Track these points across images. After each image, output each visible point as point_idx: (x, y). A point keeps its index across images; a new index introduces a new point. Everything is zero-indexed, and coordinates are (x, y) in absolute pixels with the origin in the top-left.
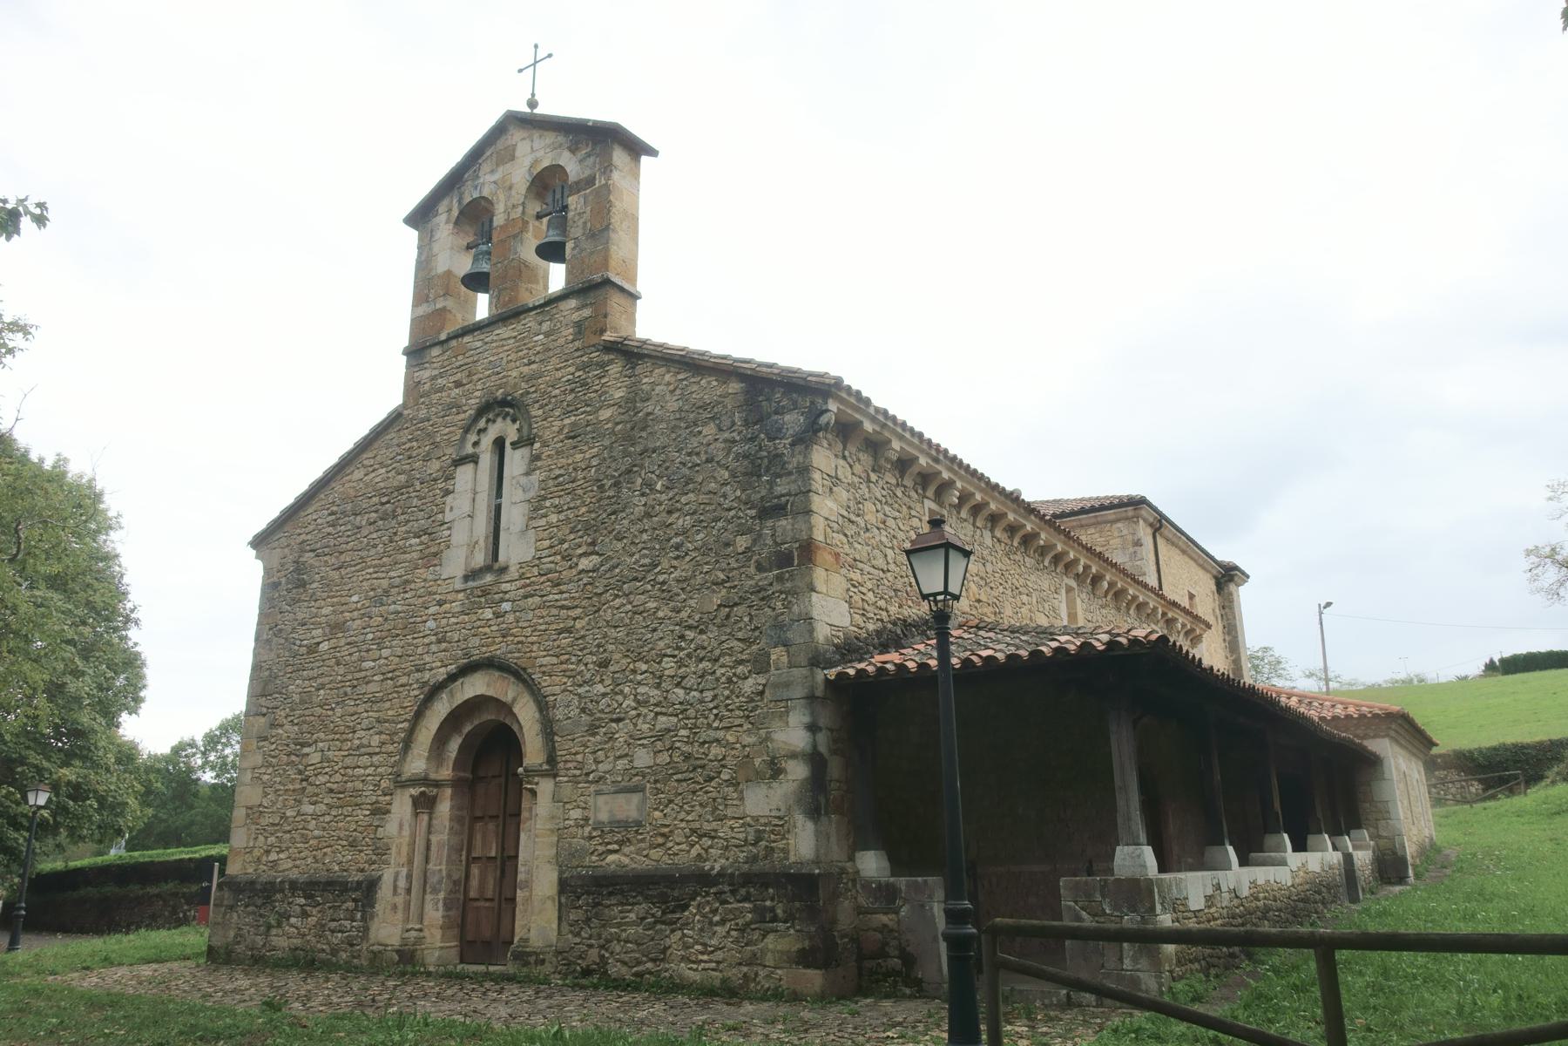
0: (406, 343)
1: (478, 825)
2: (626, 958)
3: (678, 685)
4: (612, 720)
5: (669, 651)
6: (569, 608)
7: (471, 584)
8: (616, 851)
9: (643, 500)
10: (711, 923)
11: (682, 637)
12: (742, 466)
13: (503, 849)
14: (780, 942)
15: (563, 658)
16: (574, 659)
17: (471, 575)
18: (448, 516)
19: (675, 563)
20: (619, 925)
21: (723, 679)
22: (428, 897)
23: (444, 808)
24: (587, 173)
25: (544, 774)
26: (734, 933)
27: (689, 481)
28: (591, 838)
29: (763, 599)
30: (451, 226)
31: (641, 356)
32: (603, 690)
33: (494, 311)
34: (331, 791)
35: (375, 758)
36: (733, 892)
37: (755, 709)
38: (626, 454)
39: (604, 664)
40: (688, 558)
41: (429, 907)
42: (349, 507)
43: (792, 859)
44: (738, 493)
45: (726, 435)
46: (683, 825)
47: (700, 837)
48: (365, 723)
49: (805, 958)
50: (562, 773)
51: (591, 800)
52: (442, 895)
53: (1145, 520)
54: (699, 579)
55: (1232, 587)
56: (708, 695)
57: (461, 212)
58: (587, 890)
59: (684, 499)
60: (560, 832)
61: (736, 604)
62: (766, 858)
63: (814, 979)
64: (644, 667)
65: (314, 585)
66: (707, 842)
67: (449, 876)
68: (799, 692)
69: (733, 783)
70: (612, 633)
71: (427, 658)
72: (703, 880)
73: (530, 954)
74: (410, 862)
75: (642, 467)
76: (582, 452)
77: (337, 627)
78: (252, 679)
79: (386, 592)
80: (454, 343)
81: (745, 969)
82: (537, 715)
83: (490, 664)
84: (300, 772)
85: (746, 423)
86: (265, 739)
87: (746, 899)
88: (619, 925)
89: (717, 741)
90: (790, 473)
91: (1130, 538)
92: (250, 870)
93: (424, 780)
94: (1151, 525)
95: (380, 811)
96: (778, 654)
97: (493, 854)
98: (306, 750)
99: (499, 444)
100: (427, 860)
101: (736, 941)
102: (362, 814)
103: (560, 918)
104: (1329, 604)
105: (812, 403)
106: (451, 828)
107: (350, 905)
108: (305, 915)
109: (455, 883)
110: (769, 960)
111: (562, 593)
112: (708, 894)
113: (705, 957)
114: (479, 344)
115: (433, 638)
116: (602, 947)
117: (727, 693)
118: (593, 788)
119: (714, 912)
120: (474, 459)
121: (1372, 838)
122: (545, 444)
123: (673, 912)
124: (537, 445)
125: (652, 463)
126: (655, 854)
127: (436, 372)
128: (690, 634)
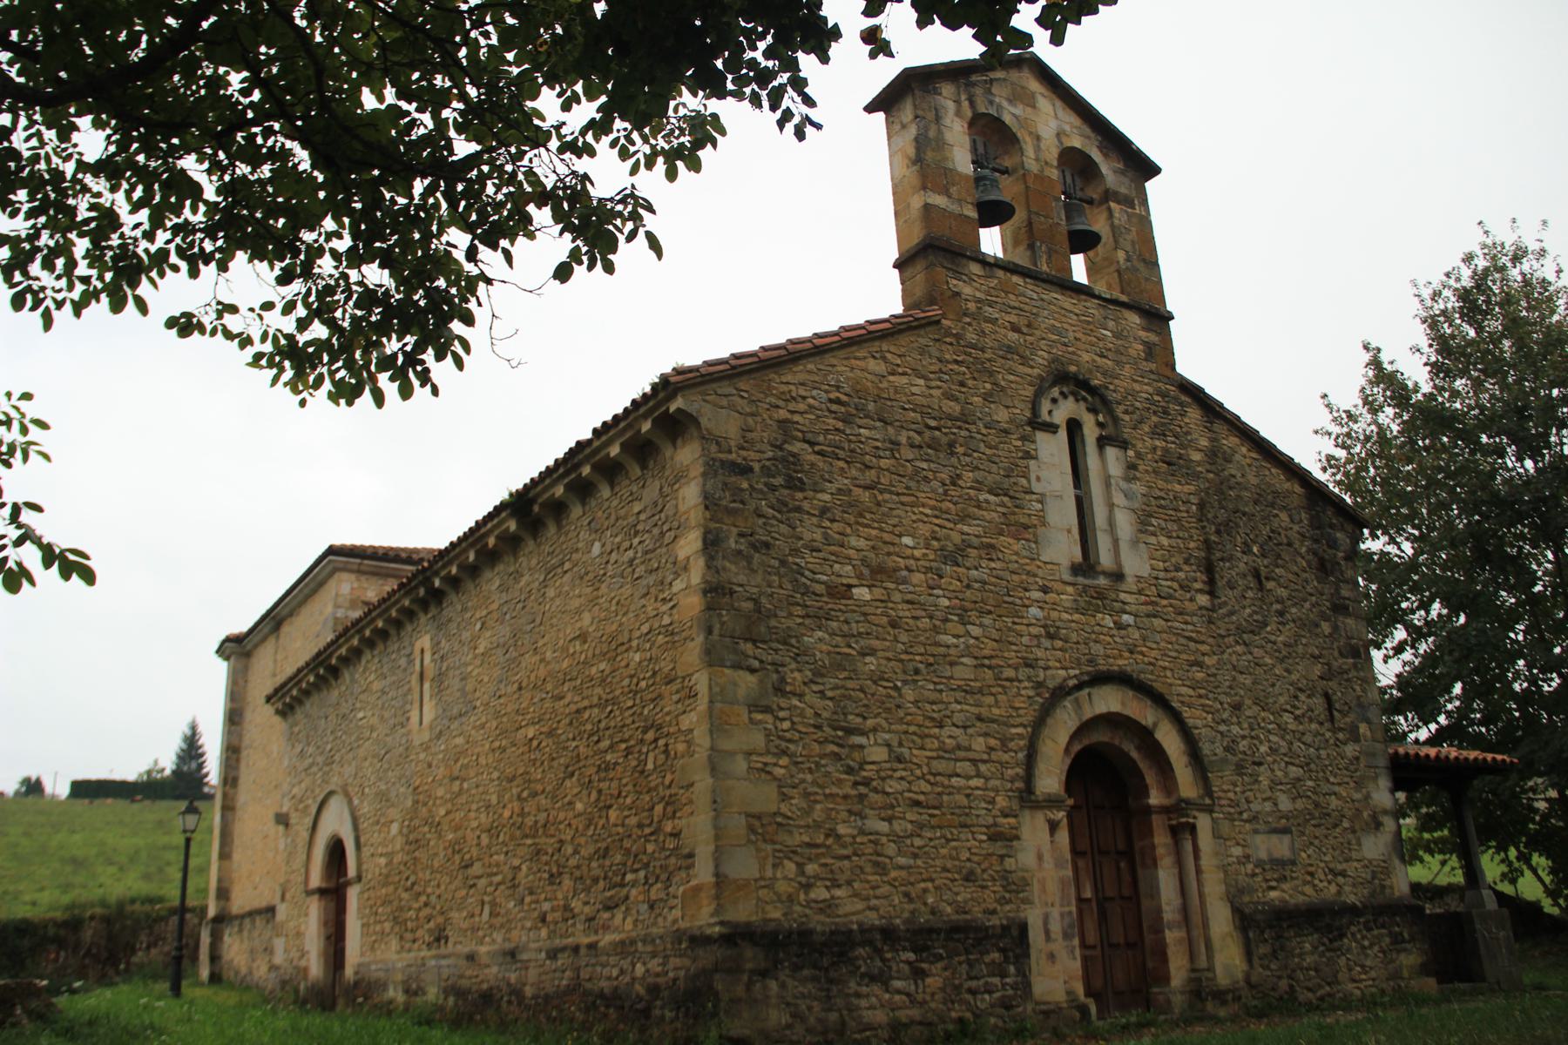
2: (1310, 984)
7: (1080, 580)
10: (1364, 948)
11: (1296, 697)
18: (1036, 487)
28: (1254, 875)
34: (917, 803)
35: (983, 768)
43: (1397, 894)
47: (1336, 875)
58: (1262, 925)
60: (1224, 868)
66: (1340, 880)
71: (1040, 653)
84: (850, 770)
86: (767, 710)
87: (1383, 926)
92: (777, 915)
95: (1005, 838)
96: (1363, 728)
103: (1249, 955)
107: (996, 956)
108: (918, 974)
111: (1186, 623)
124: (1131, 453)
128: (1302, 697)
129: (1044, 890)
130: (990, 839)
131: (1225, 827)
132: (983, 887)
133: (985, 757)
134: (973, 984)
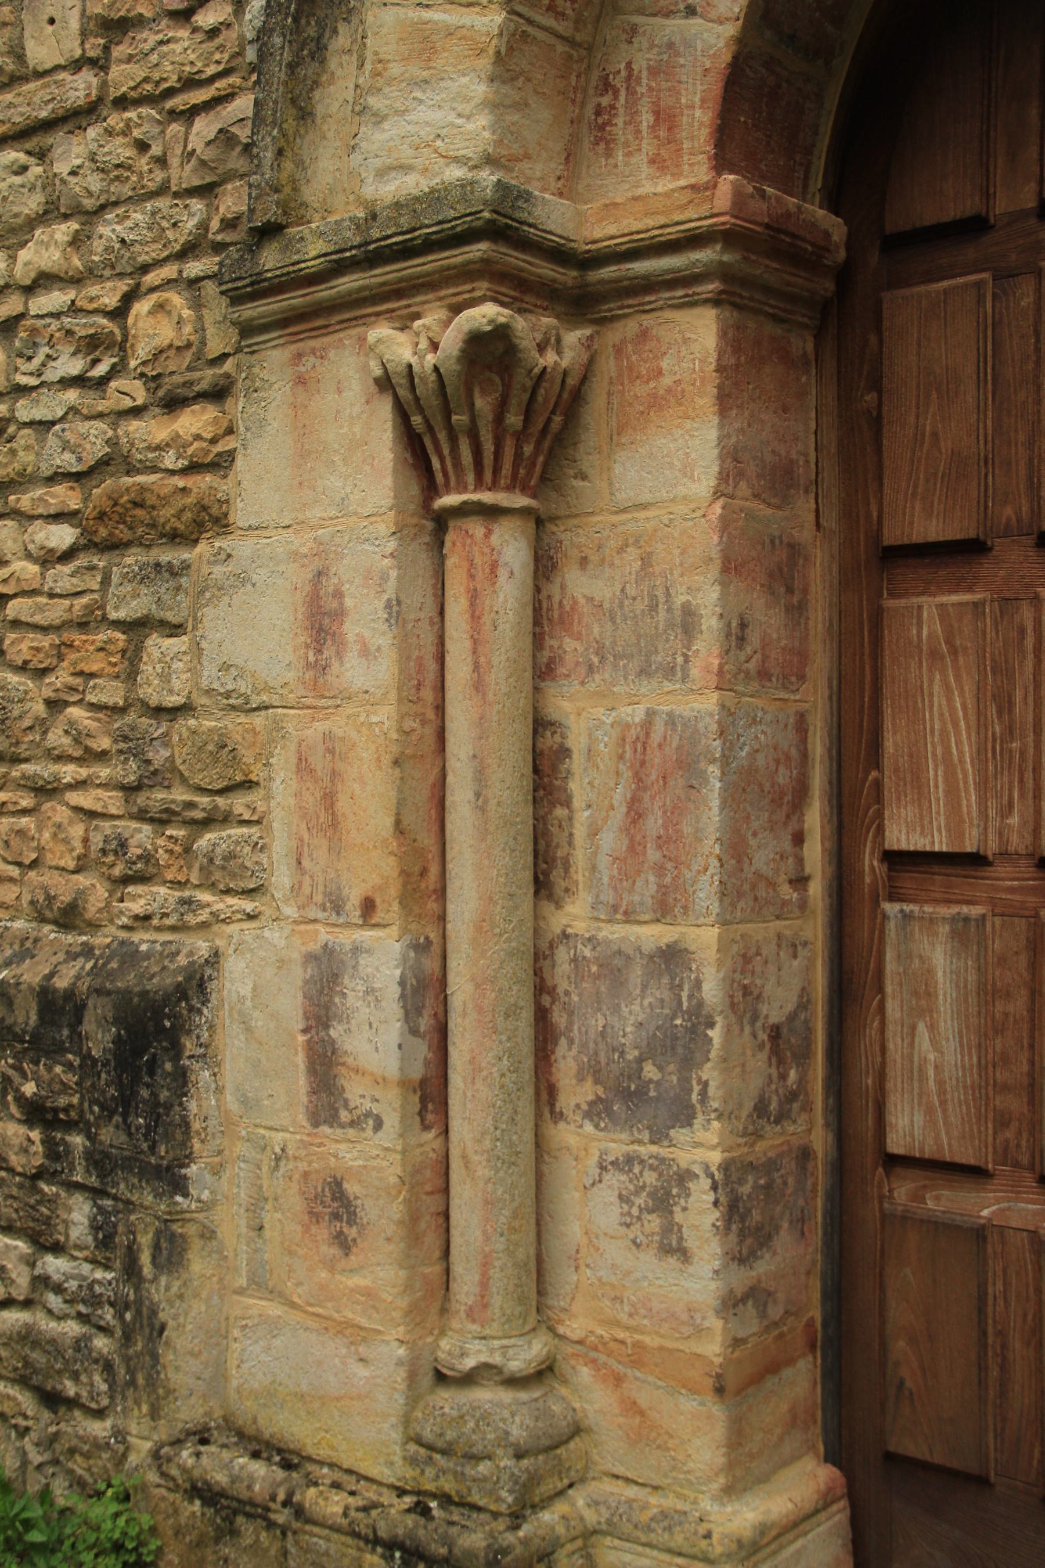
1: (929, 613)
22: (583, 1142)
35: (71, 152)
41: (594, 1213)
52: (702, 1147)
67: (744, 1000)
74: (424, 885)
95: (149, 526)
100: (544, 874)
106: (737, 634)
109: (780, 1043)
129: (328, 816)
130: (88, 544)
132: (47, 791)
133: (80, 87)
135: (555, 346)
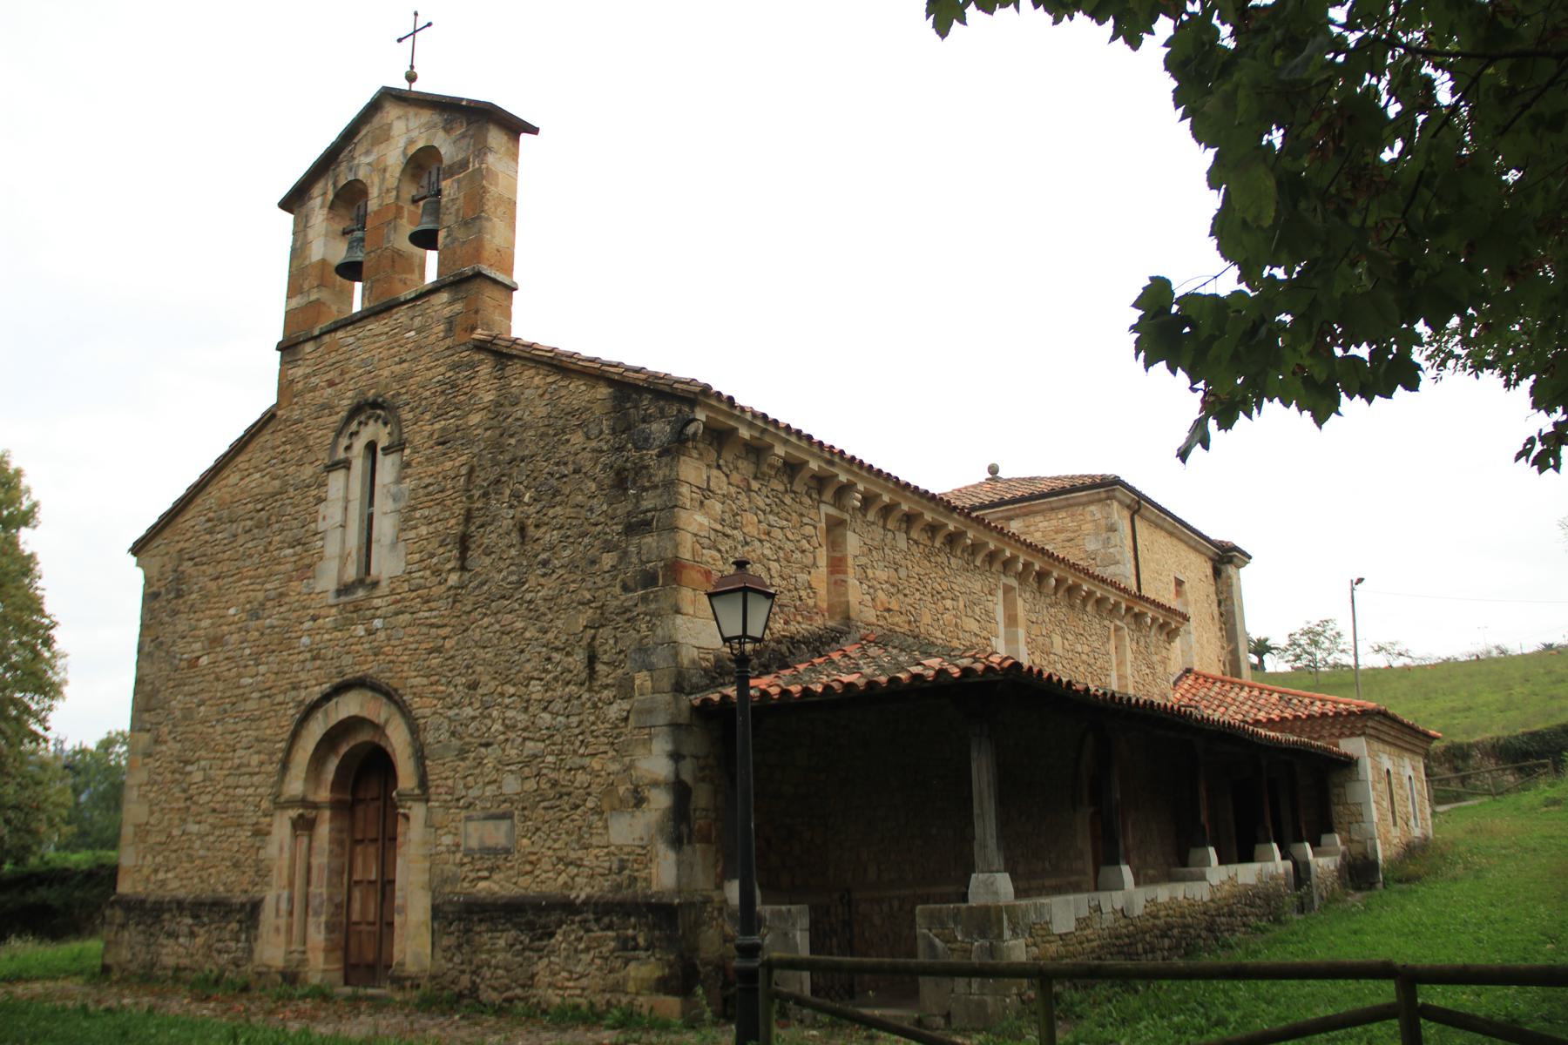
0: (280, 338)
1: (359, 849)
3: (545, 709)
4: (481, 745)
5: (535, 674)
6: (438, 627)
7: (343, 599)
8: (486, 878)
9: (511, 512)
10: (576, 950)
11: (549, 659)
12: (608, 478)
13: (383, 874)
14: (644, 970)
15: (434, 678)
16: (444, 680)
17: (344, 590)
18: (321, 526)
19: (542, 581)
20: (489, 951)
21: (589, 704)
22: (311, 920)
23: (324, 830)
24: (460, 157)
25: (417, 799)
26: (598, 961)
27: (556, 493)
28: (462, 865)
29: (628, 621)
30: (325, 211)
31: (511, 357)
32: (472, 713)
33: (367, 305)
34: (214, 810)
35: (255, 778)
36: (597, 920)
37: (619, 735)
38: (495, 463)
39: (473, 686)
40: (555, 576)
41: (311, 930)
42: (225, 513)
43: (654, 888)
44: (605, 507)
45: (594, 444)
46: (550, 853)
48: (245, 742)
49: (663, 986)
50: (433, 797)
51: (461, 826)
52: (323, 918)
53: (1120, 502)
54: (565, 599)
55: (1231, 569)
56: (574, 720)
57: (337, 196)
58: (460, 916)
59: (551, 512)
61: (602, 626)
62: (629, 886)
63: (671, 1005)
64: (512, 690)
65: (194, 596)
66: (573, 870)
67: (330, 899)
68: (662, 719)
69: (597, 811)
70: (481, 654)
71: (303, 676)
72: (566, 907)
73: (408, 978)
74: (291, 884)
75: (510, 476)
76: (451, 459)
77: (216, 641)
78: (135, 693)
79: (262, 605)
80: (327, 338)
81: (608, 996)
82: (408, 738)
83: (361, 683)
84: (184, 791)
85: (614, 431)
86: (150, 755)
87: (610, 927)
88: (489, 951)
89: (583, 768)
90: (656, 487)
91: (1103, 522)
93: (303, 802)
94: (1128, 507)
95: (260, 833)
96: (642, 679)
97: (373, 877)
98: (189, 768)
99: (371, 447)
100: (308, 883)
101: (600, 969)
102: (244, 835)
104: (1360, 580)
105: (679, 411)
106: (331, 852)
108: (192, 935)
109: (338, 906)
110: (631, 987)
112: (573, 922)
113: (571, 984)
114: (351, 340)
115: (308, 655)
116: (474, 973)
117: (592, 718)
118: (463, 813)
119: (580, 939)
120: (346, 465)
121: (1343, 843)
122: (415, 451)
123: (540, 939)
124: (407, 451)
125: (520, 473)
126: (525, 881)
127: (309, 370)
128: (557, 656)
129: (280, 874)
131: (439, 816)
134: (220, 945)
135: (311, 813)
